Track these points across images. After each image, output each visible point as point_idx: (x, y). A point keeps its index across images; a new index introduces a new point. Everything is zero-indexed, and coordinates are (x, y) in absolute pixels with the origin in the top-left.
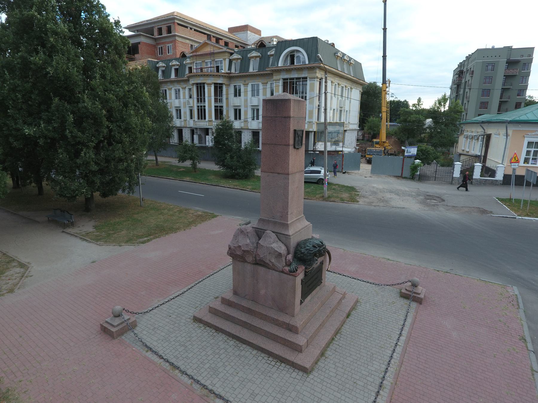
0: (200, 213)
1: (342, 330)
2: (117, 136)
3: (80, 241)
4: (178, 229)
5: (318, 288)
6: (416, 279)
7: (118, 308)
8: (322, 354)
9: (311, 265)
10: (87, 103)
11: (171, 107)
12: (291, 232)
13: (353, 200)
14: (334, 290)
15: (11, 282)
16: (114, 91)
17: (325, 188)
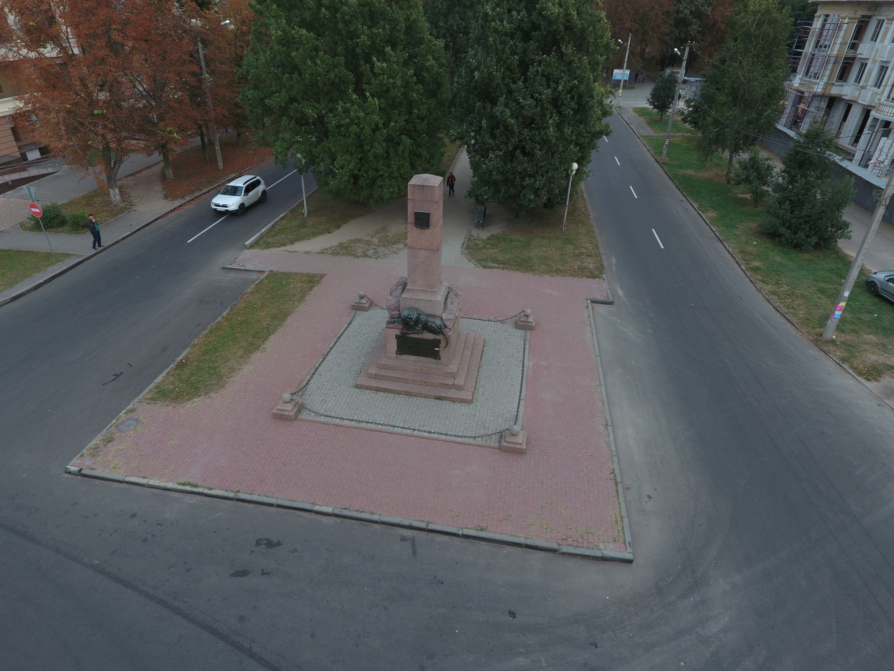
0: (591, 266)
1: (415, 398)
2: (529, 146)
3: (462, 242)
4: (532, 271)
5: (433, 360)
6: (517, 428)
7: (362, 293)
8: (378, 390)
9: (408, 329)
10: (498, 110)
11: (875, 62)
12: (404, 296)
13: (873, 373)
14: (453, 376)
15: (387, 252)
16: (540, 94)
17: (832, 324)
